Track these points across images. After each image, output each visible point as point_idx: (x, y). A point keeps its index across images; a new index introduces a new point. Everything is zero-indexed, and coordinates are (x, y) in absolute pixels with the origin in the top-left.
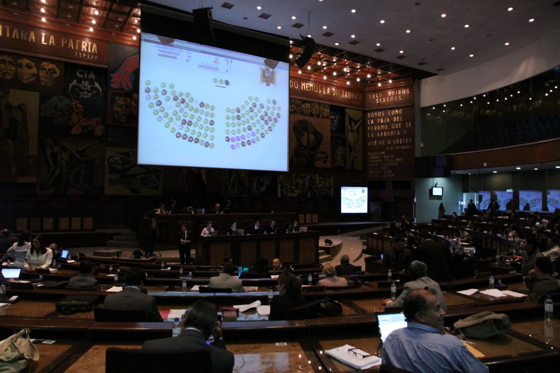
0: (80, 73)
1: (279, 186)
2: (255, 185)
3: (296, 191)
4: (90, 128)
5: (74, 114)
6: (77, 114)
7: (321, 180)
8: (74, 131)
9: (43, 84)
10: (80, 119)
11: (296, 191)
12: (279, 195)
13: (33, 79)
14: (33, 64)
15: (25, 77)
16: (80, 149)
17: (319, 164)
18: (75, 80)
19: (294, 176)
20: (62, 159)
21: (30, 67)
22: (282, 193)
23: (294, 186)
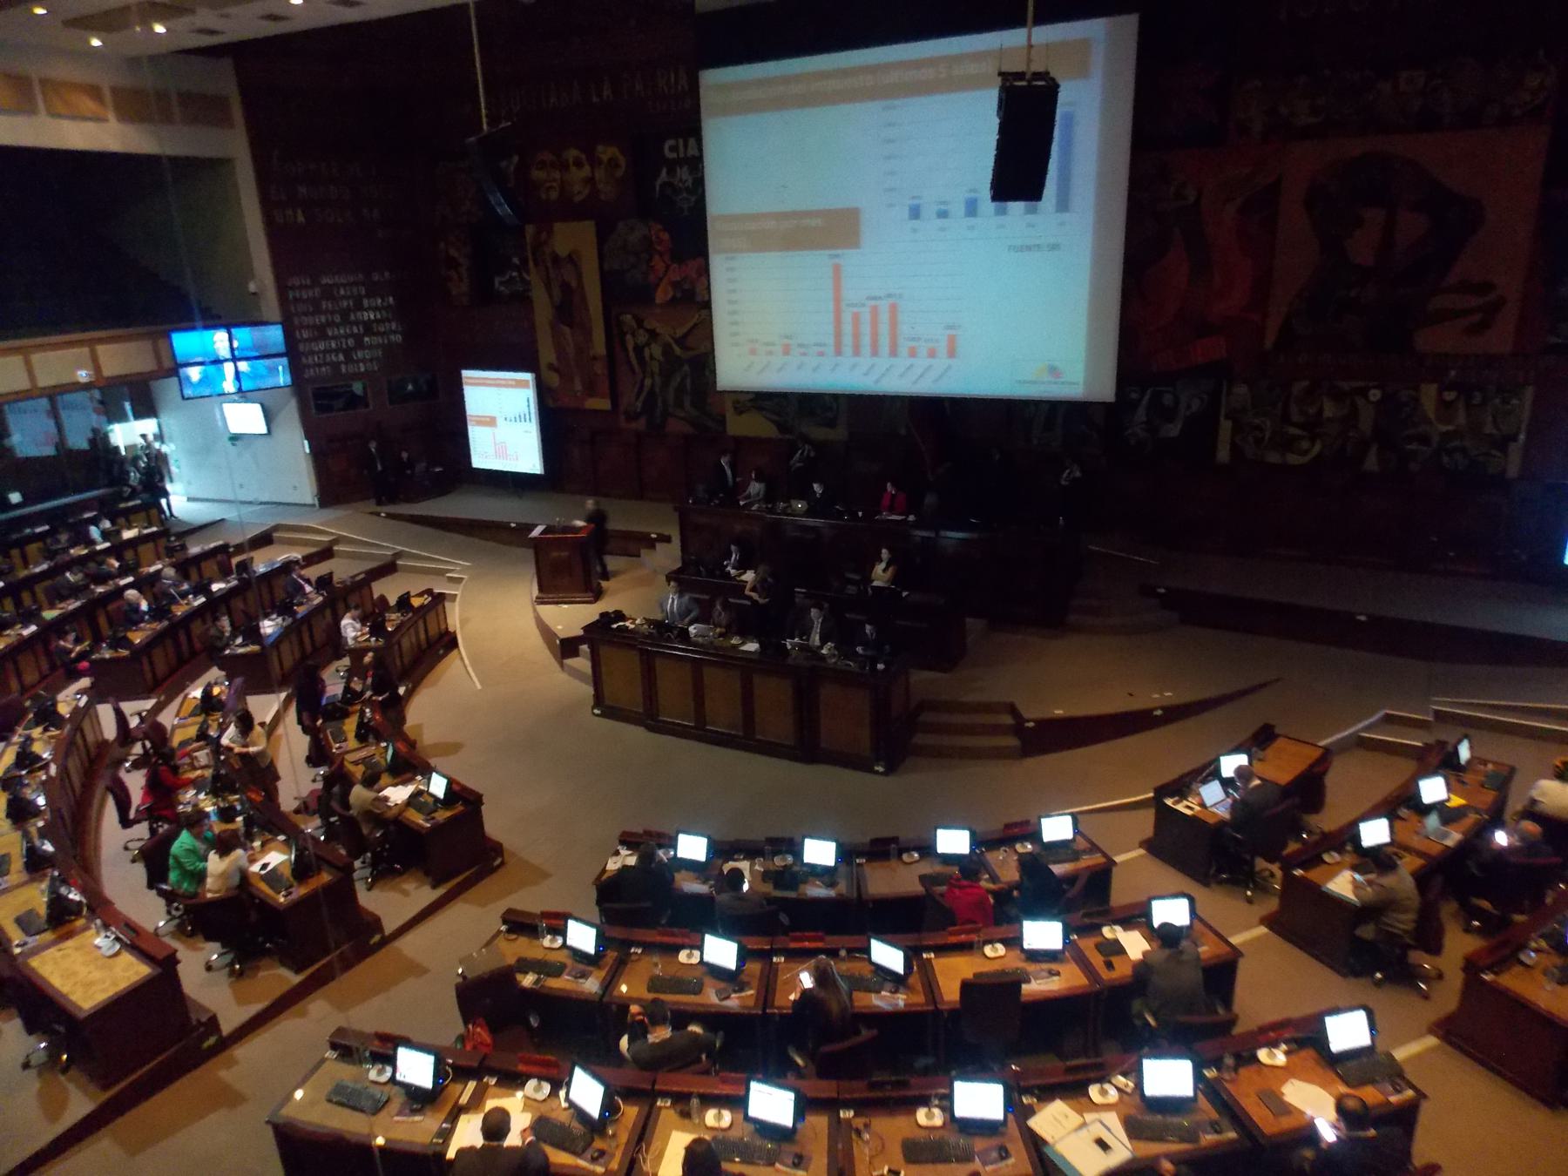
0: (674, 149)
1: (1226, 426)
2: (1141, 414)
3: (1305, 445)
4: (686, 286)
5: (657, 257)
6: (661, 254)
7: (1448, 405)
8: (661, 296)
9: (603, 197)
10: (668, 267)
11: (1305, 445)
12: (1223, 454)
13: (586, 192)
14: (583, 157)
15: (577, 188)
16: (680, 332)
17: (1426, 340)
18: (664, 171)
19: (1299, 387)
20: (652, 357)
21: (578, 164)
22: (1234, 447)
23: (1296, 425)
